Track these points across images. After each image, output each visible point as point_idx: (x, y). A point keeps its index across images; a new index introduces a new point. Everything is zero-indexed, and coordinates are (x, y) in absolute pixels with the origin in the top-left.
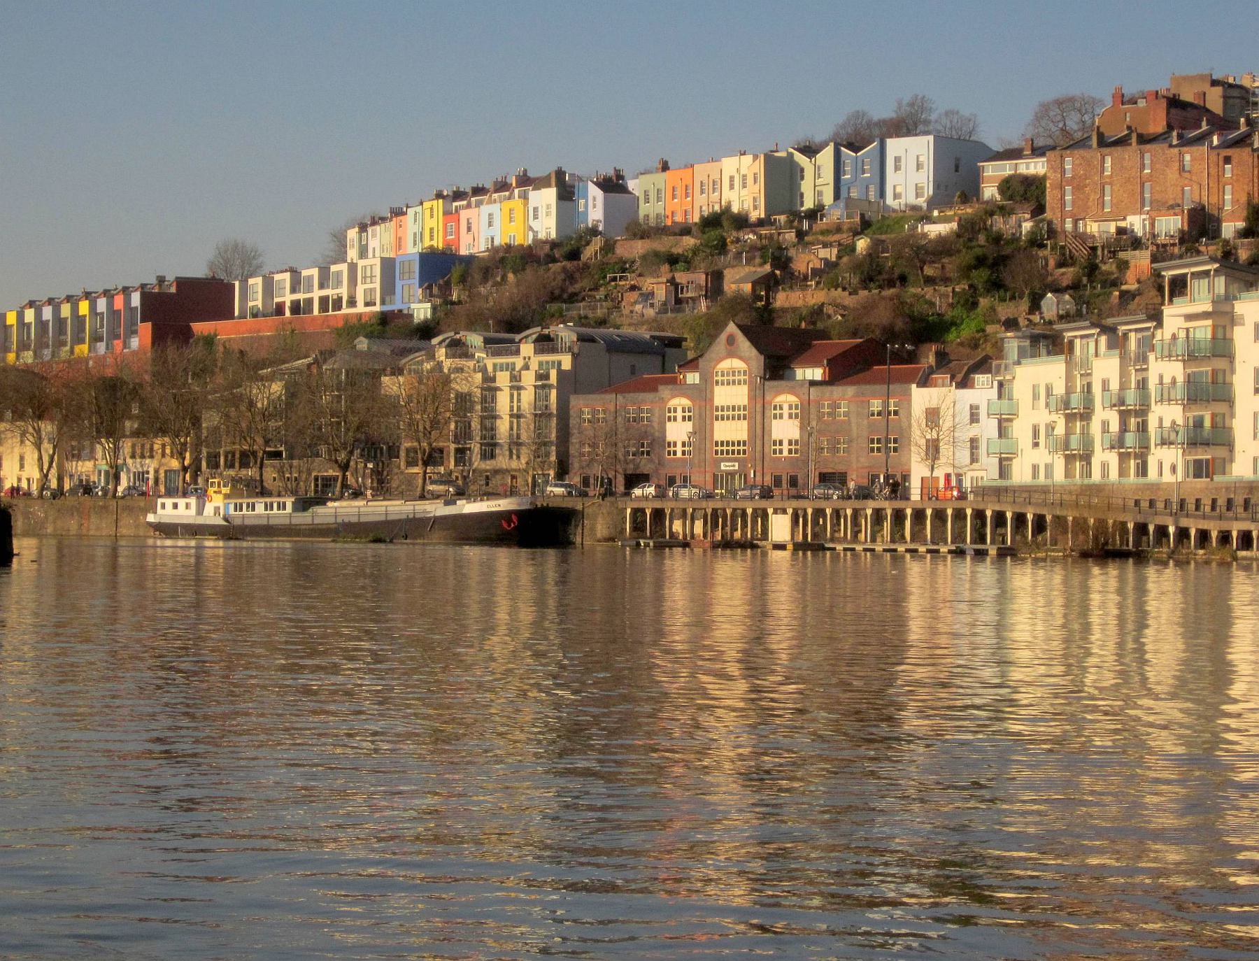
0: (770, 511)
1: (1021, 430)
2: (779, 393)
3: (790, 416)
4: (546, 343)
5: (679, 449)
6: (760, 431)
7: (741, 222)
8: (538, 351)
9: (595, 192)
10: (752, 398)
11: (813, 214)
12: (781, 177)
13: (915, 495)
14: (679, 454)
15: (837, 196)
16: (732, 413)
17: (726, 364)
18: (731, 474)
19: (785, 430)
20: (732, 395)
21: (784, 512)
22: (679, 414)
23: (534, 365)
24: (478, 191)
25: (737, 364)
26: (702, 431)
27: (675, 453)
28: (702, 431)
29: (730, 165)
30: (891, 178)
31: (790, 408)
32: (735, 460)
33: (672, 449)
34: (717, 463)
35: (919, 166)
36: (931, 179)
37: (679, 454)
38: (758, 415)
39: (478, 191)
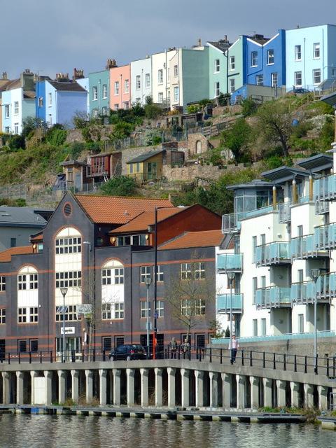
0: (32, 373)
1: (246, 284)
2: (106, 259)
3: (117, 282)
5: (28, 315)
6: (92, 296)
7: (151, 111)
9: (49, 89)
10: (86, 262)
11: (224, 100)
12: (193, 64)
14: (28, 320)
15: (245, 81)
16: (68, 280)
18: (69, 338)
19: (113, 293)
20: (69, 262)
21: (40, 374)
22: (28, 282)
25: (73, 232)
27: (25, 320)
29: (159, 59)
30: (292, 66)
31: (117, 272)
34: (59, 326)
35: (317, 53)
36: (326, 64)
38: (91, 281)
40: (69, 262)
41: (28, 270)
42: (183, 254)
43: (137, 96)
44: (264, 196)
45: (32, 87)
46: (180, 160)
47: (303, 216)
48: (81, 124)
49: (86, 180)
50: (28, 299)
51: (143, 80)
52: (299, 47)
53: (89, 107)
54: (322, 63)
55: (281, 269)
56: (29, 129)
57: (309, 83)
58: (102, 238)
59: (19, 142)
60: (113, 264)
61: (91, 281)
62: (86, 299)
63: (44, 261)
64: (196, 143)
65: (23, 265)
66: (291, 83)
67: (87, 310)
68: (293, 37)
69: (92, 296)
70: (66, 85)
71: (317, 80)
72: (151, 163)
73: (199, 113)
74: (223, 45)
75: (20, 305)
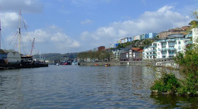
1: (145, 55)
4: (119, 50)
6: (132, 56)
7: (138, 40)
11: (144, 39)
12: (141, 36)
17: (130, 51)
19: (134, 55)
20: (131, 53)
24: (122, 39)
26: (129, 56)
28: (129, 56)
29: (138, 36)
30: (149, 36)
38: (132, 55)
39: (122, 39)
40: (131, 53)
41: (127, 54)
42: (140, 52)
43: (136, 39)
44: (146, 47)
45: (128, 38)
46: (140, 44)
47: (150, 49)
48: (132, 42)
50: (127, 56)
53: (132, 40)
54: (152, 36)
55: (148, 53)
56: (127, 42)
57: (151, 38)
58: (133, 51)
59: (127, 43)
60: (134, 53)
61: (132, 55)
63: (129, 53)
64: (141, 43)
66: (149, 38)
68: (149, 34)
69: (132, 56)
70: (130, 38)
72: (137, 45)
73: (141, 40)
74: (144, 35)
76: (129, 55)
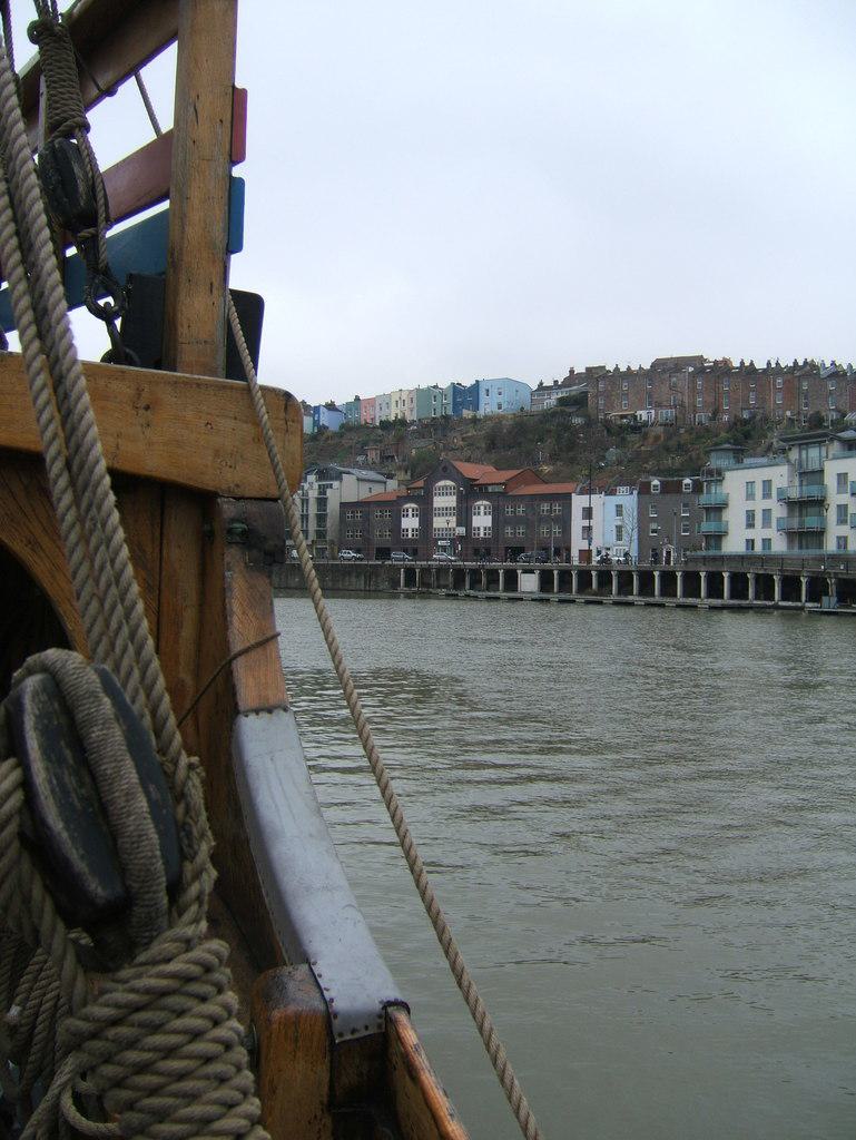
0: (519, 572)
3: (485, 514)
8: (320, 479)
13: (575, 561)
14: (410, 536)
16: (445, 511)
20: (444, 501)
21: (531, 572)
23: (316, 486)
25: (449, 483)
28: (426, 521)
32: (445, 539)
33: (477, 532)
37: (410, 536)
38: (464, 515)
40: (440, 502)
41: (410, 506)
49: (382, 457)
50: (410, 523)
51: (384, 406)
52: (488, 390)
60: (482, 504)
61: (464, 515)
62: (459, 524)
65: (406, 503)
67: (461, 531)
71: (500, 408)
75: (403, 526)
76: (426, 516)
